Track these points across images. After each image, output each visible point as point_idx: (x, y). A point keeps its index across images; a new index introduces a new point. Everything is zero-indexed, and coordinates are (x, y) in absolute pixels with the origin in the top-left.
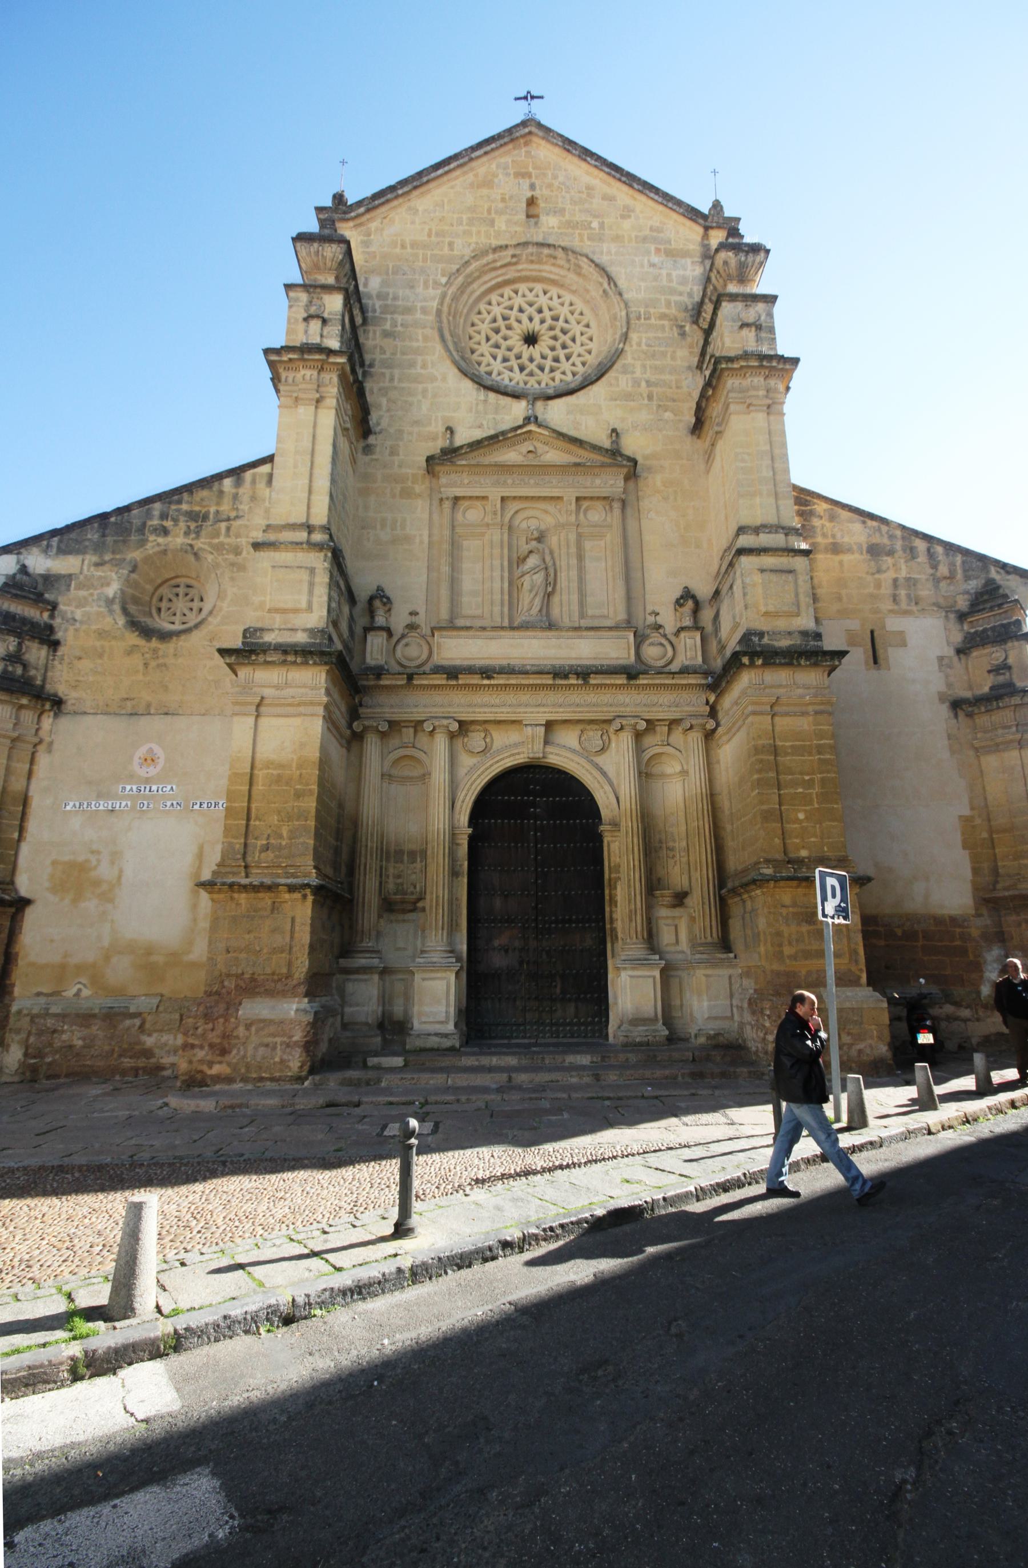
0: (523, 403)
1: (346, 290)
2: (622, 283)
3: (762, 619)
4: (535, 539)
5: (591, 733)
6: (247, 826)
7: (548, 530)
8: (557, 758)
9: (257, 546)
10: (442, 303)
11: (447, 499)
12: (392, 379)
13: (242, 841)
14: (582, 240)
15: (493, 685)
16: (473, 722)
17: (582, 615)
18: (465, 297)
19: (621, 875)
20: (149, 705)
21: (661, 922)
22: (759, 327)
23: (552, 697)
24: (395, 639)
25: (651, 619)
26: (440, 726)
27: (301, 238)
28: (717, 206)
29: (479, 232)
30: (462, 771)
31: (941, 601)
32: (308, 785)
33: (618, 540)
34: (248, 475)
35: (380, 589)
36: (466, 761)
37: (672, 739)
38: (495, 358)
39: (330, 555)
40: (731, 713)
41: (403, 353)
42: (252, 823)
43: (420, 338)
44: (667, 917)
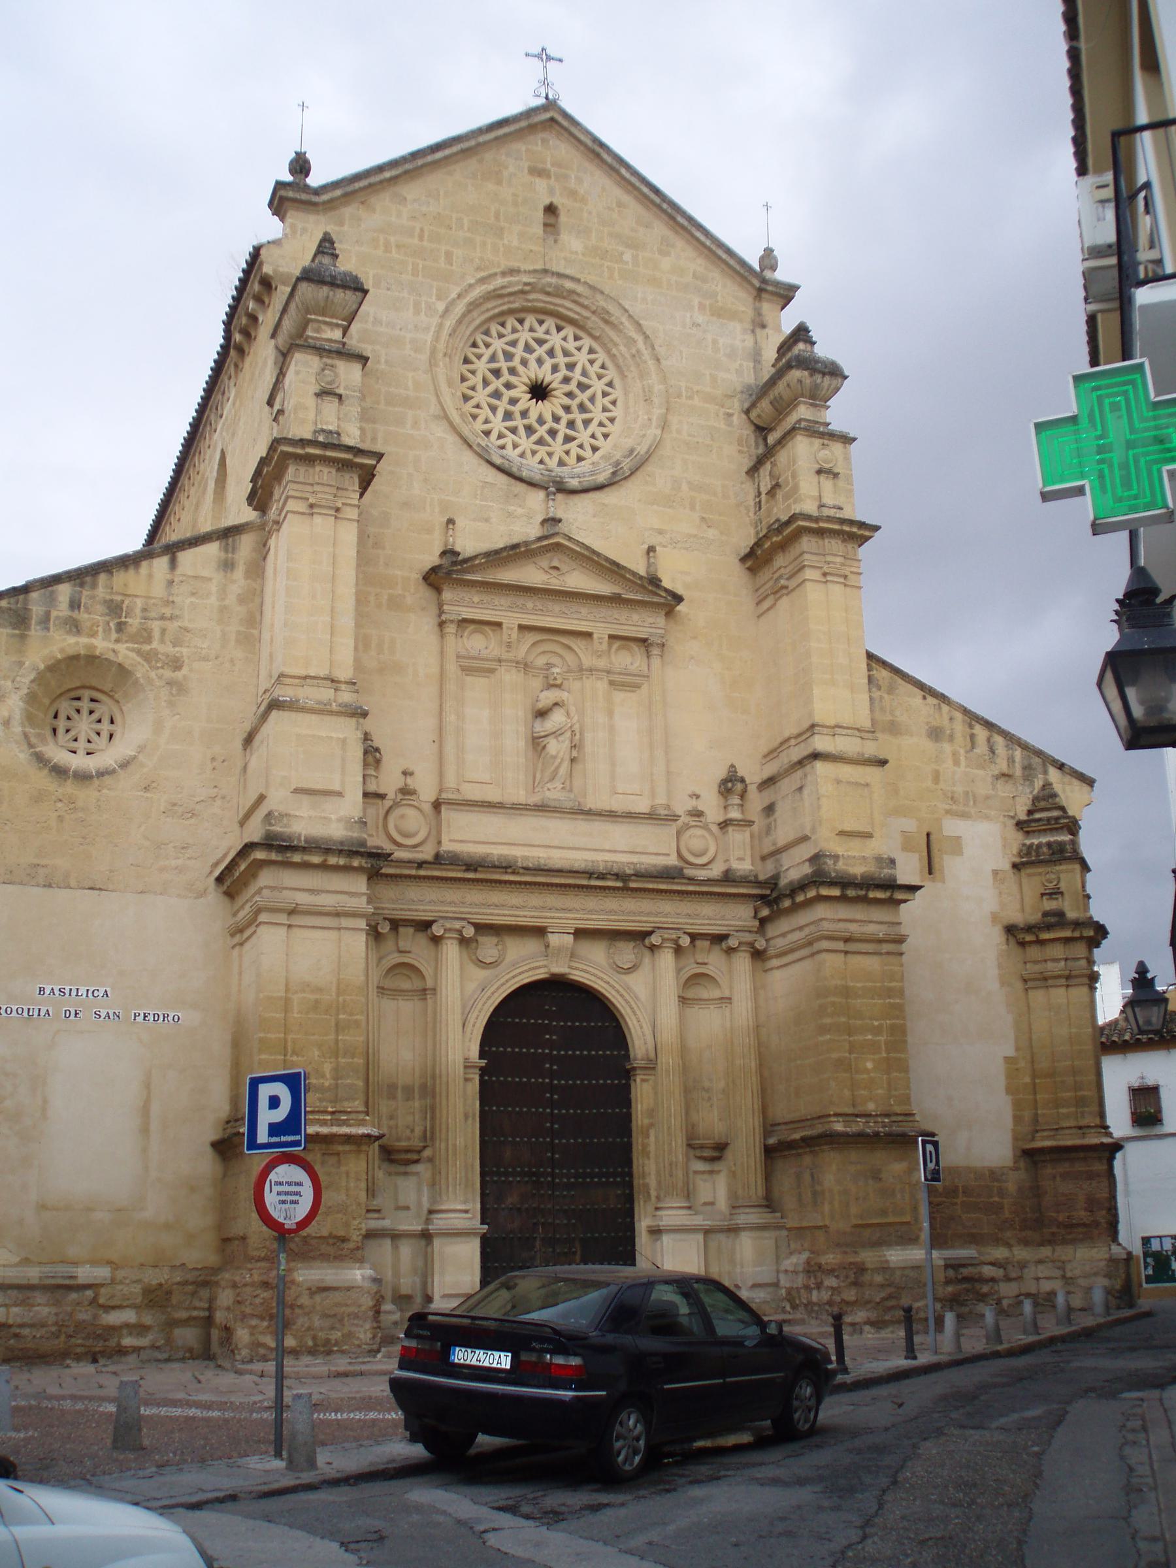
0: (541, 494)
10: (437, 338)
11: (452, 621)
14: (611, 277)
25: (691, 804)
28: (769, 258)
29: (484, 244)
32: (351, 1014)
43: (410, 384)
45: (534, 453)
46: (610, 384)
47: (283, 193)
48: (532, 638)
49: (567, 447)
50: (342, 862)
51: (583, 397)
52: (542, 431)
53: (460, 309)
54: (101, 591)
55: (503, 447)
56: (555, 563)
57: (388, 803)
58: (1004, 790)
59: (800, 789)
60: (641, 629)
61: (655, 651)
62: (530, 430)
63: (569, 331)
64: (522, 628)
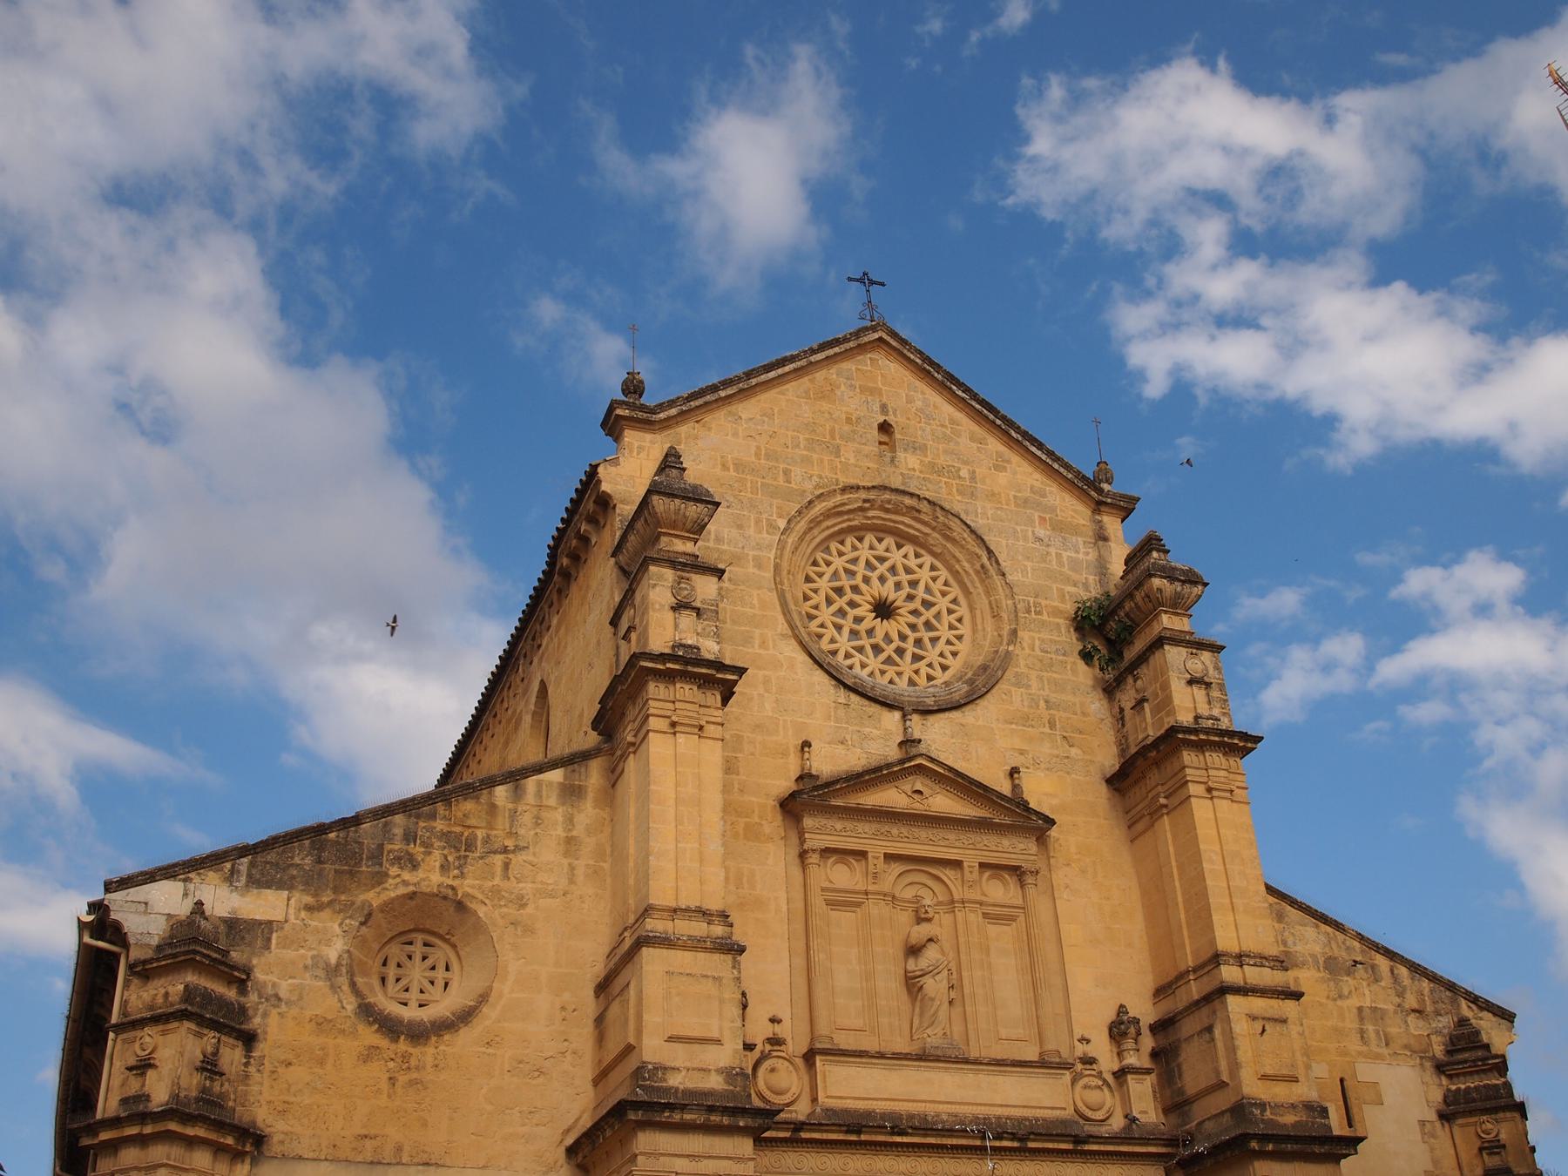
0: (897, 715)
20: (399, 1149)
25: (1080, 1049)
29: (822, 461)
31: (1412, 1042)
34: (531, 783)
45: (883, 672)
46: (954, 601)
47: (619, 412)
48: (897, 868)
49: (916, 666)
50: (726, 1120)
51: (928, 615)
52: (889, 650)
53: (802, 525)
55: (851, 667)
56: (918, 787)
57: (756, 1053)
58: (1416, 1026)
59: (1210, 1029)
61: (1029, 880)
62: (877, 649)
63: (909, 549)
64: (889, 857)
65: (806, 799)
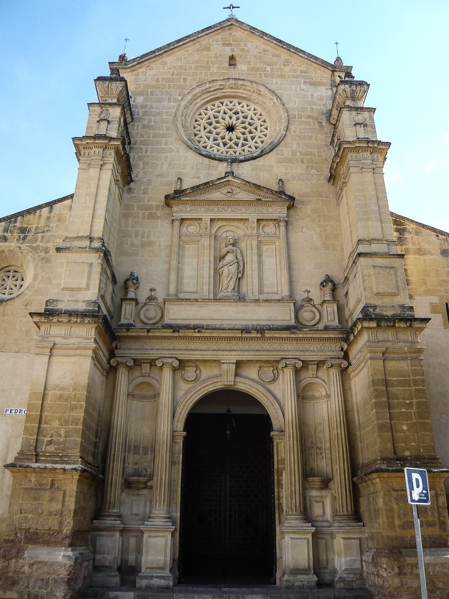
0: (225, 164)
1: (123, 106)
2: (285, 99)
3: (375, 297)
4: (231, 244)
5: (266, 369)
6: (39, 427)
7: (239, 239)
8: (243, 385)
9: (58, 250)
10: (177, 110)
12: (146, 152)
13: (35, 437)
14: (261, 77)
15: (202, 337)
16: (188, 361)
17: (261, 292)
18: (192, 106)
19: (285, 466)
21: (313, 500)
22: (365, 125)
23: (241, 345)
24: (140, 305)
25: (305, 295)
26: (166, 363)
27: (100, 79)
28: (338, 59)
29: (201, 73)
30: (180, 393)
32: (79, 401)
33: (284, 245)
34: (57, 207)
35: (132, 274)
36: (183, 387)
37: (320, 374)
38: (209, 139)
39: (102, 255)
40: (358, 357)
41: (154, 137)
42: (42, 425)
44: (317, 496)
54: (18, 225)
55: (213, 151)
60: (274, 215)
65: (174, 197)
